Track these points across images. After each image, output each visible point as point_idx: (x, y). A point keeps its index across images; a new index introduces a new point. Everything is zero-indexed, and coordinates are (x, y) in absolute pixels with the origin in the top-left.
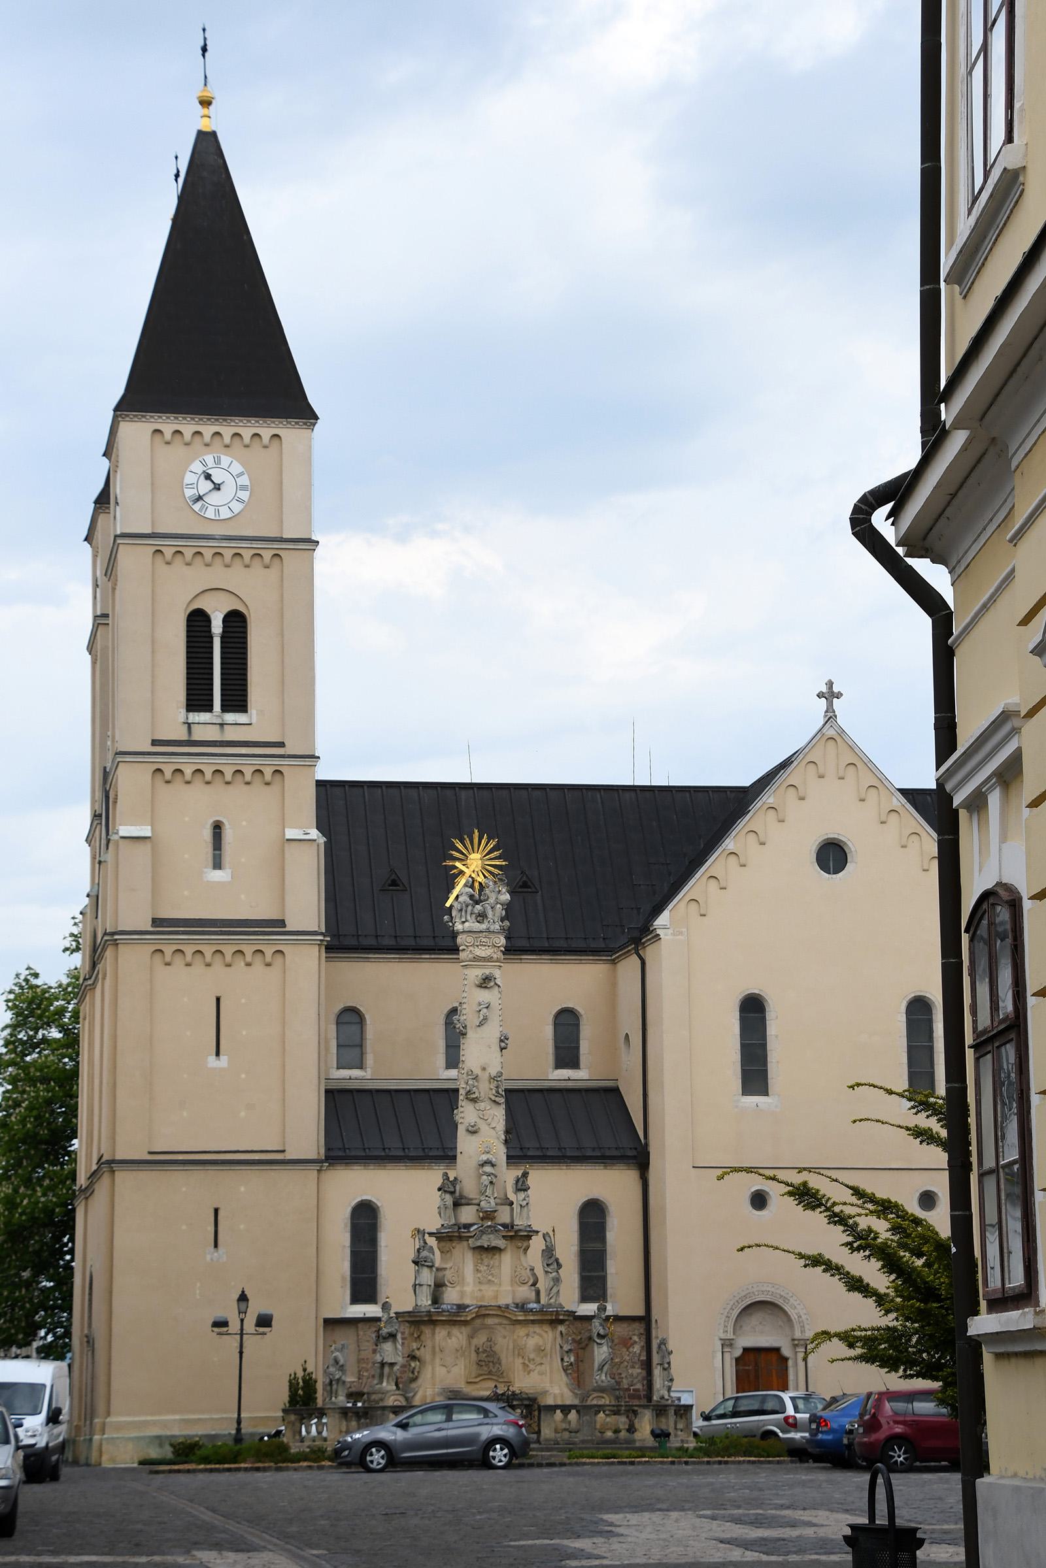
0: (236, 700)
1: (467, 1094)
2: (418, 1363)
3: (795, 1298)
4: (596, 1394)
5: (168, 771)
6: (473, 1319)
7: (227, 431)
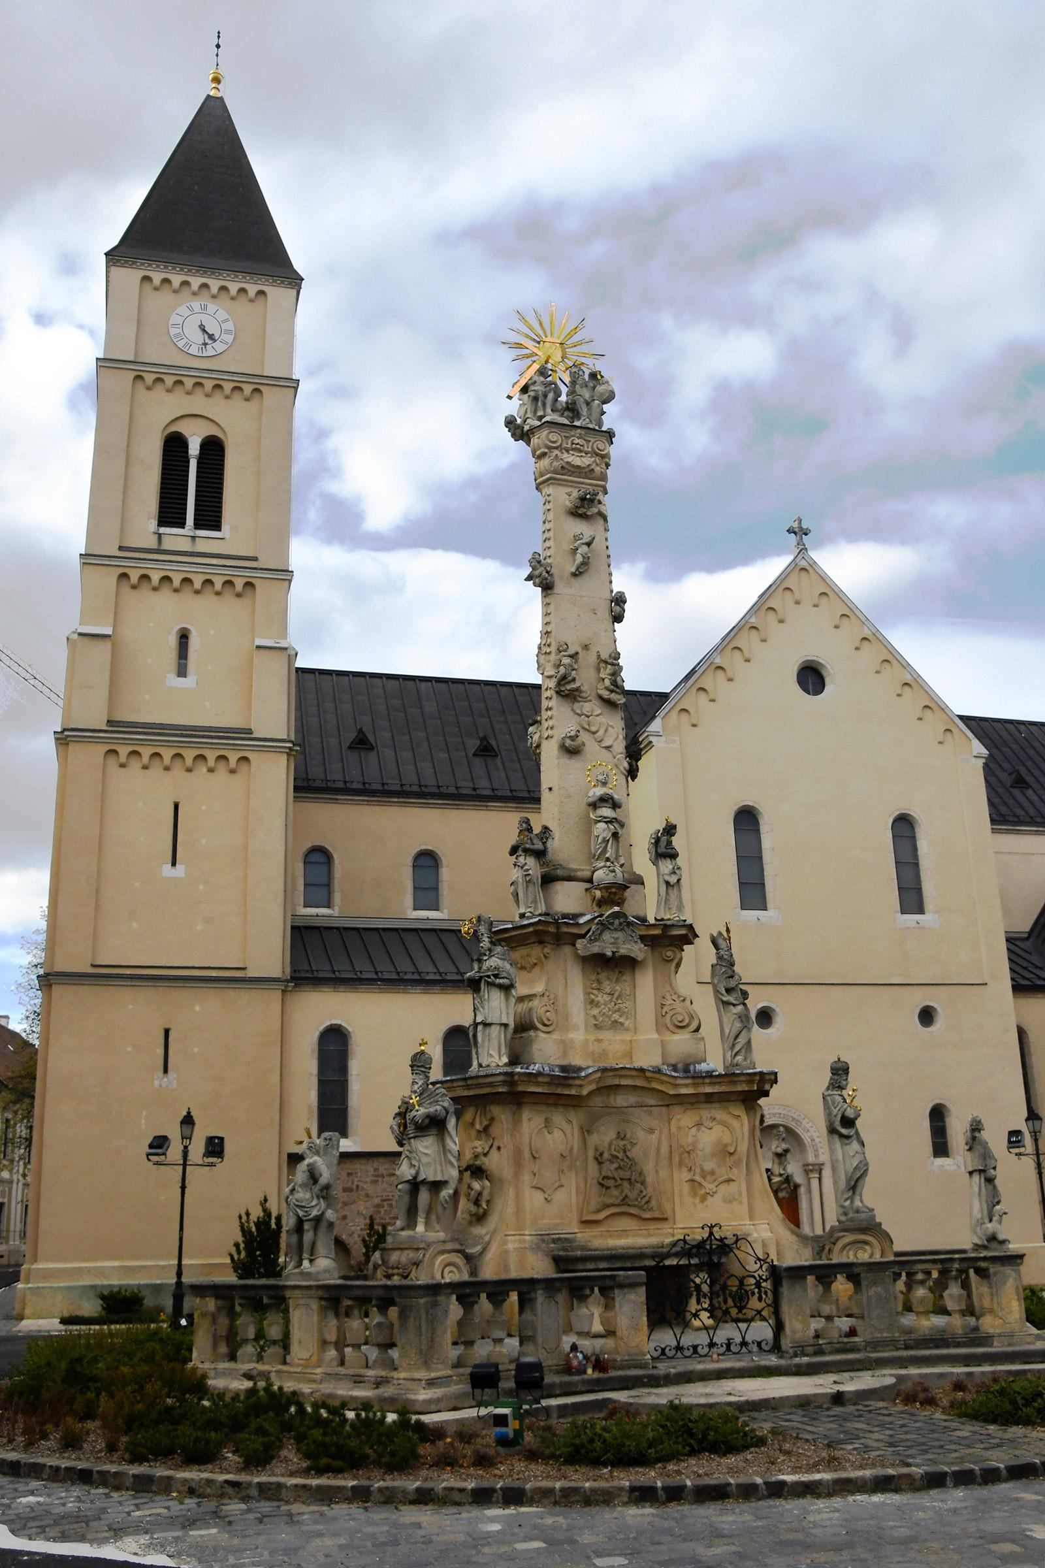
0: (210, 517)
1: (559, 684)
2: (487, 1183)
3: (807, 1120)
4: (850, 1238)
5: (134, 576)
6: (591, 1093)
7: (215, 284)
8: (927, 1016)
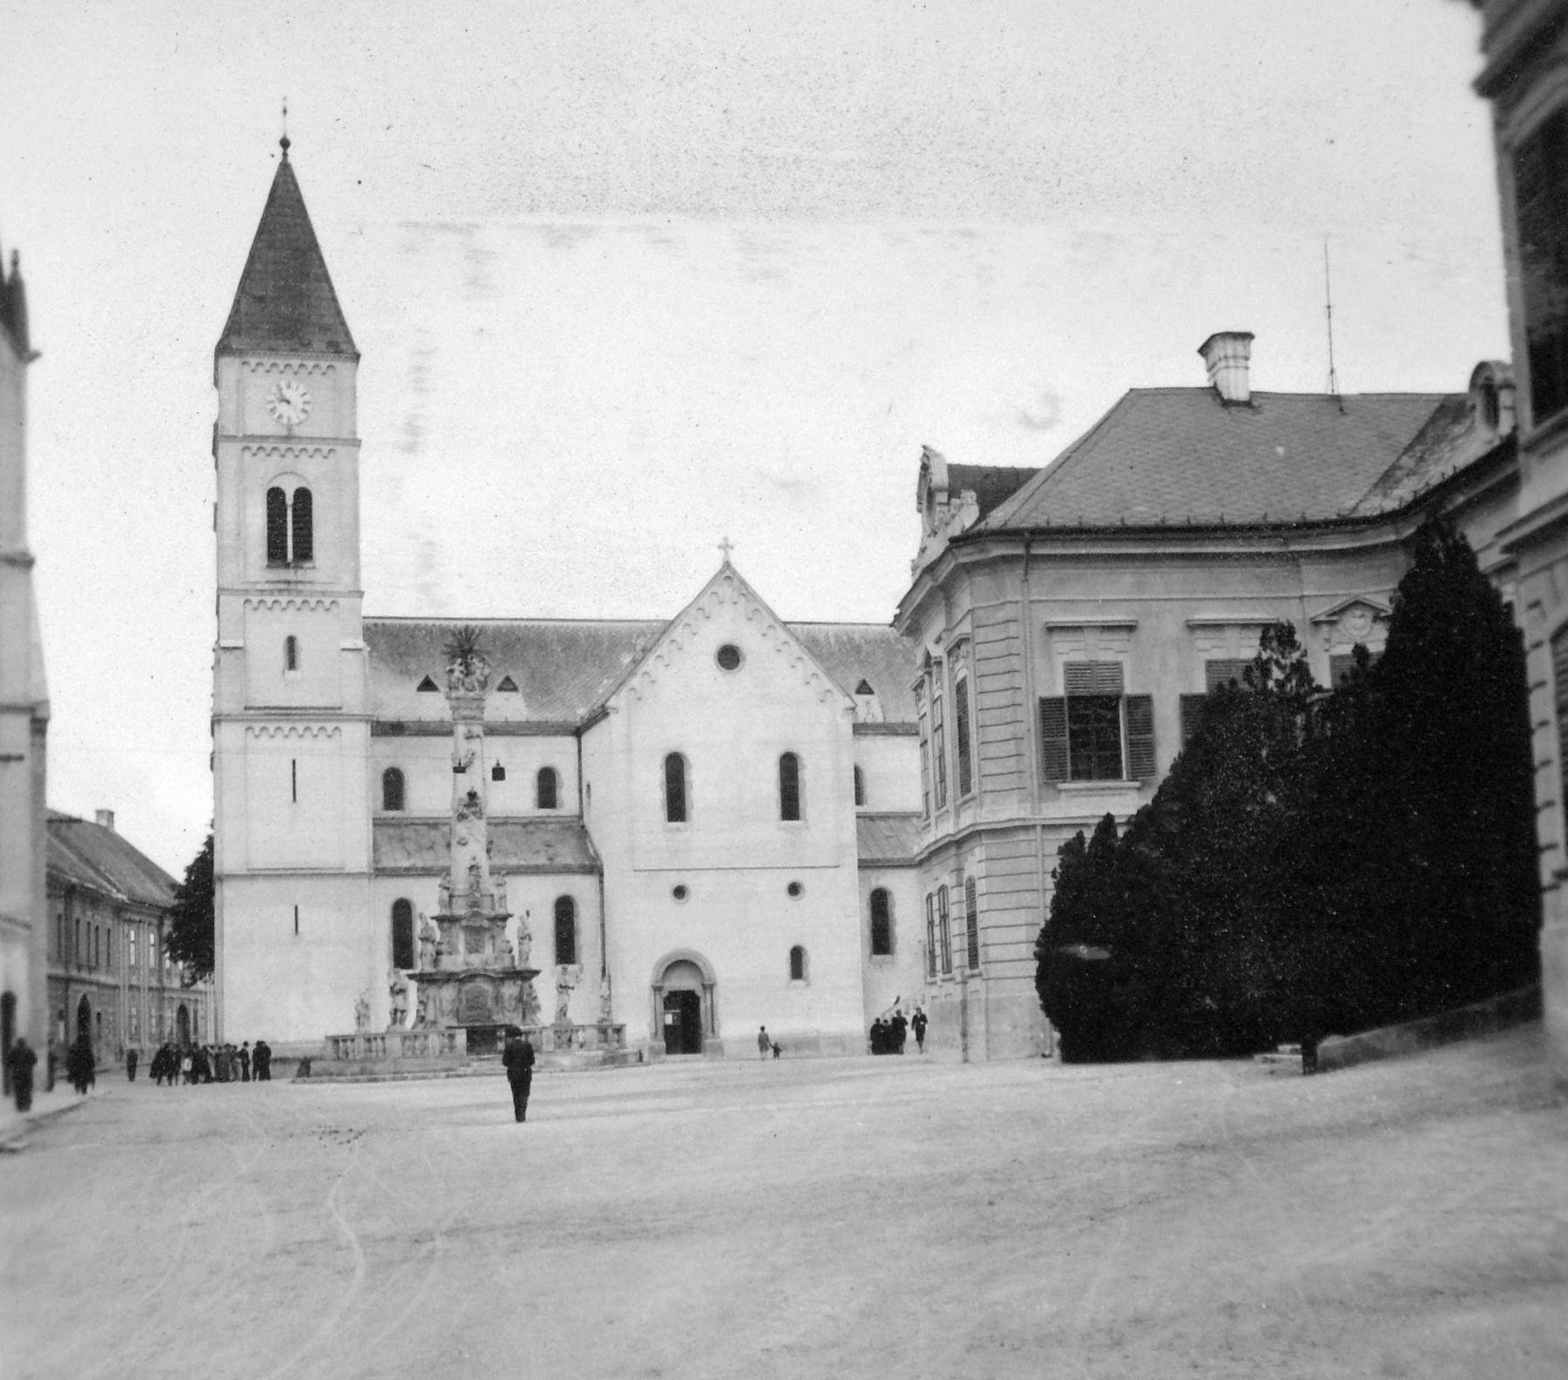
0: (304, 552)
8: (794, 889)
